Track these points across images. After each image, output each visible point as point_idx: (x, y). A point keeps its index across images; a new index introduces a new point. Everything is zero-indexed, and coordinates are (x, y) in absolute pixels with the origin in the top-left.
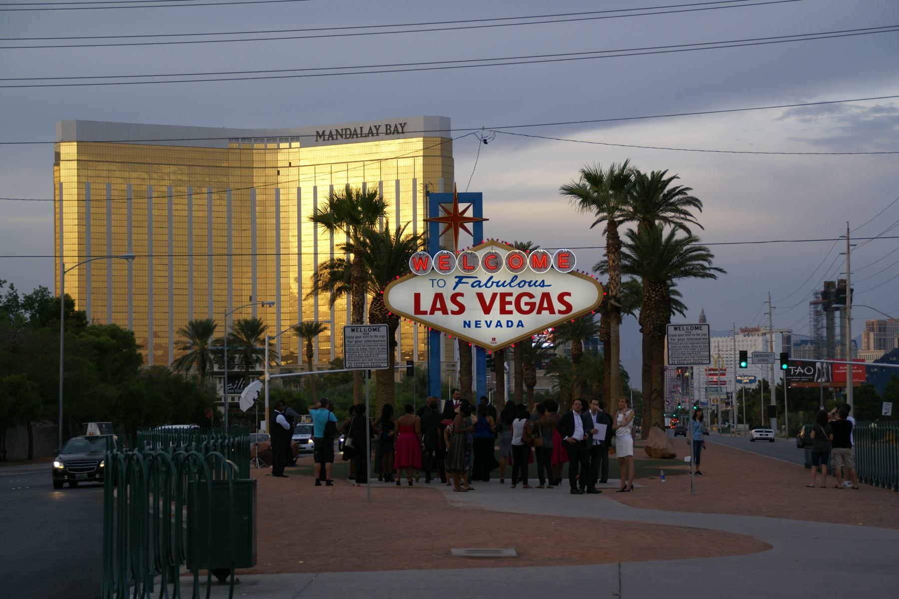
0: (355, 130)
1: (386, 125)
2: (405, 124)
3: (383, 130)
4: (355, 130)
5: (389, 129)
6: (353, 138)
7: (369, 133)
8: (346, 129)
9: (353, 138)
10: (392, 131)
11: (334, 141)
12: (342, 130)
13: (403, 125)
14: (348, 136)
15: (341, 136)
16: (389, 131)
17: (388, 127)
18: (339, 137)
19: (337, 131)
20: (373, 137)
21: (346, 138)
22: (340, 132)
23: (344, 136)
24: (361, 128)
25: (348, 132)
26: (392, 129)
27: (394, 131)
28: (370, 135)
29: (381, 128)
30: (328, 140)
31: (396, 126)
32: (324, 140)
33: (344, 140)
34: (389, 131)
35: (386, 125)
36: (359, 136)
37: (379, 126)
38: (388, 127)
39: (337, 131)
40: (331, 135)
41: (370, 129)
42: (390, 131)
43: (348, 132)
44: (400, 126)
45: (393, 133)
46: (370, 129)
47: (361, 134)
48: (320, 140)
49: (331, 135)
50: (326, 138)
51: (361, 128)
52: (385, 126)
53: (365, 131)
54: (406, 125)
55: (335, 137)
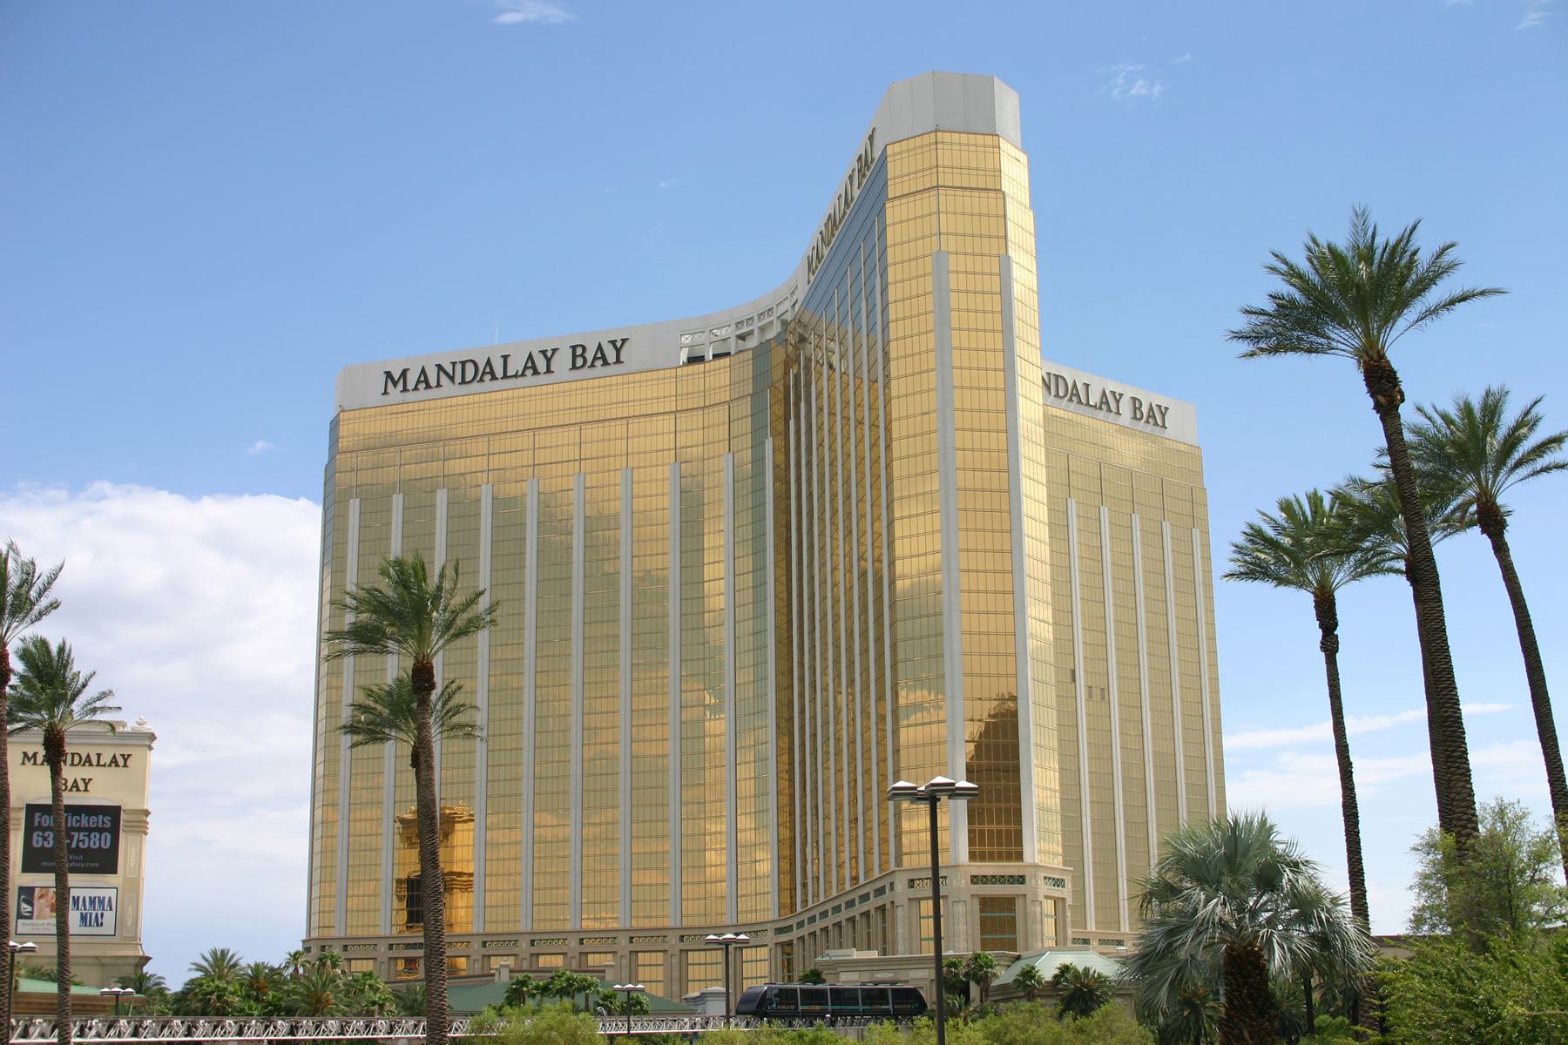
0: (489, 362)
1: (574, 348)
2: (624, 341)
3: (562, 361)
4: (489, 362)
5: (582, 355)
6: (481, 380)
7: (526, 368)
8: (463, 363)
9: (481, 380)
10: (589, 363)
11: (429, 391)
12: (454, 364)
13: (619, 345)
14: (469, 375)
15: (452, 378)
16: (579, 362)
17: (579, 351)
18: (443, 378)
19: (440, 367)
20: (536, 377)
21: (463, 382)
22: (449, 369)
23: (458, 378)
24: (505, 358)
25: (470, 369)
26: (590, 356)
27: (595, 358)
29: (557, 354)
30: (416, 389)
31: (600, 347)
32: (405, 390)
33: (457, 389)
34: (579, 362)
35: (574, 348)
36: (499, 374)
37: (554, 351)
38: (579, 351)
39: (440, 367)
41: (530, 357)
42: (585, 360)
43: (470, 369)
44: (611, 346)
45: (592, 365)
46: (530, 357)
47: (505, 376)
50: (411, 385)
51: (505, 358)
52: (571, 350)
53: (516, 365)
54: (627, 343)
55: (433, 382)
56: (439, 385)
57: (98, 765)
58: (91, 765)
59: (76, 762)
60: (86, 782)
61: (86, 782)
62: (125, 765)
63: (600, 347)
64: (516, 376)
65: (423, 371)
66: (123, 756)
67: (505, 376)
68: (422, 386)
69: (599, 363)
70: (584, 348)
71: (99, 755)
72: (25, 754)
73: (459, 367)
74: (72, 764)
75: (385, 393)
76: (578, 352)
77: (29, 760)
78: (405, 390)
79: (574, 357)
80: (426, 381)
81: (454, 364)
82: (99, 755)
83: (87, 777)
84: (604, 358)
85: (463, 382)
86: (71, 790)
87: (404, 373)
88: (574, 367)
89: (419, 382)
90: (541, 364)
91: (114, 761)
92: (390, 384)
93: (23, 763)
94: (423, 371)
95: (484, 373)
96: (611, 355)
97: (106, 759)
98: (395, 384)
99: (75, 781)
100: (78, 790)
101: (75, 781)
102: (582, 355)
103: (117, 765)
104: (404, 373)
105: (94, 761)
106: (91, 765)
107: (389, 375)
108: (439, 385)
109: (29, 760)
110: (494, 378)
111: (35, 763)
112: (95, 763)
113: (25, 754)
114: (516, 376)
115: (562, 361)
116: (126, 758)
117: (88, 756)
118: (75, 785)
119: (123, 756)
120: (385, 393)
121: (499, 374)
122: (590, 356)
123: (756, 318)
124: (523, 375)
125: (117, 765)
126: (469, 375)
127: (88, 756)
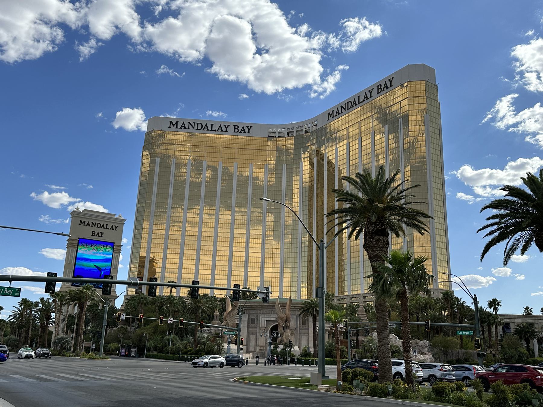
0: (206, 125)
1: (235, 126)
3: (231, 129)
4: (206, 125)
6: (204, 130)
7: (219, 129)
8: (198, 124)
9: (204, 130)
10: (239, 131)
12: (194, 123)
14: (200, 127)
15: (194, 127)
16: (236, 130)
18: (190, 127)
21: (197, 129)
23: (196, 128)
24: (212, 125)
25: (200, 125)
26: (240, 129)
27: (241, 130)
28: (220, 130)
30: (181, 128)
31: (243, 127)
32: (177, 128)
33: (194, 131)
35: (235, 126)
36: (210, 129)
38: (236, 127)
39: (189, 123)
40: (183, 125)
41: (220, 126)
43: (200, 125)
44: (247, 128)
46: (220, 126)
47: (212, 130)
48: (173, 128)
49: (183, 125)
50: (179, 127)
51: (212, 125)
53: (216, 127)
55: (187, 127)
56: (189, 128)
57: (106, 228)
58: (104, 228)
59: (99, 226)
60: (102, 234)
61: (102, 234)
62: (116, 230)
63: (243, 127)
64: (215, 131)
65: (184, 123)
66: (115, 226)
67: (212, 130)
68: (183, 128)
69: (243, 132)
70: (238, 127)
71: (107, 225)
72: (81, 221)
73: (196, 125)
74: (97, 227)
75: (170, 127)
76: (236, 128)
77: (82, 223)
78: (177, 128)
79: (235, 129)
80: (184, 126)
81: (194, 123)
82: (107, 225)
83: (102, 232)
84: (244, 131)
85: (197, 129)
86: (96, 236)
87: (177, 123)
88: (235, 132)
89: (182, 126)
90: (224, 129)
91: (112, 228)
92: (171, 125)
93: (80, 224)
94: (184, 123)
95: (204, 128)
96: (247, 131)
97: (109, 227)
98: (173, 125)
99: (98, 233)
100: (99, 236)
101: (98, 233)
102: (237, 129)
103: (113, 229)
104: (177, 123)
105: (105, 227)
106: (104, 228)
107: (171, 122)
108: (189, 128)
109: (82, 223)
110: (208, 130)
111: (84, 225)
112: (105, 227)
113: (81, 221)
114: (215, 131)
115: (231, 129)
116: (116, 227)
117: (103, 225)
118: (98, 234)
119: (115, 226)
120: (170, 127)
121: (210, 129)
122: (240, 129)
123: (295, 128)
124: (218, 131)
125: (113, 229)
126: (200, 127)
127: (103, 225)
